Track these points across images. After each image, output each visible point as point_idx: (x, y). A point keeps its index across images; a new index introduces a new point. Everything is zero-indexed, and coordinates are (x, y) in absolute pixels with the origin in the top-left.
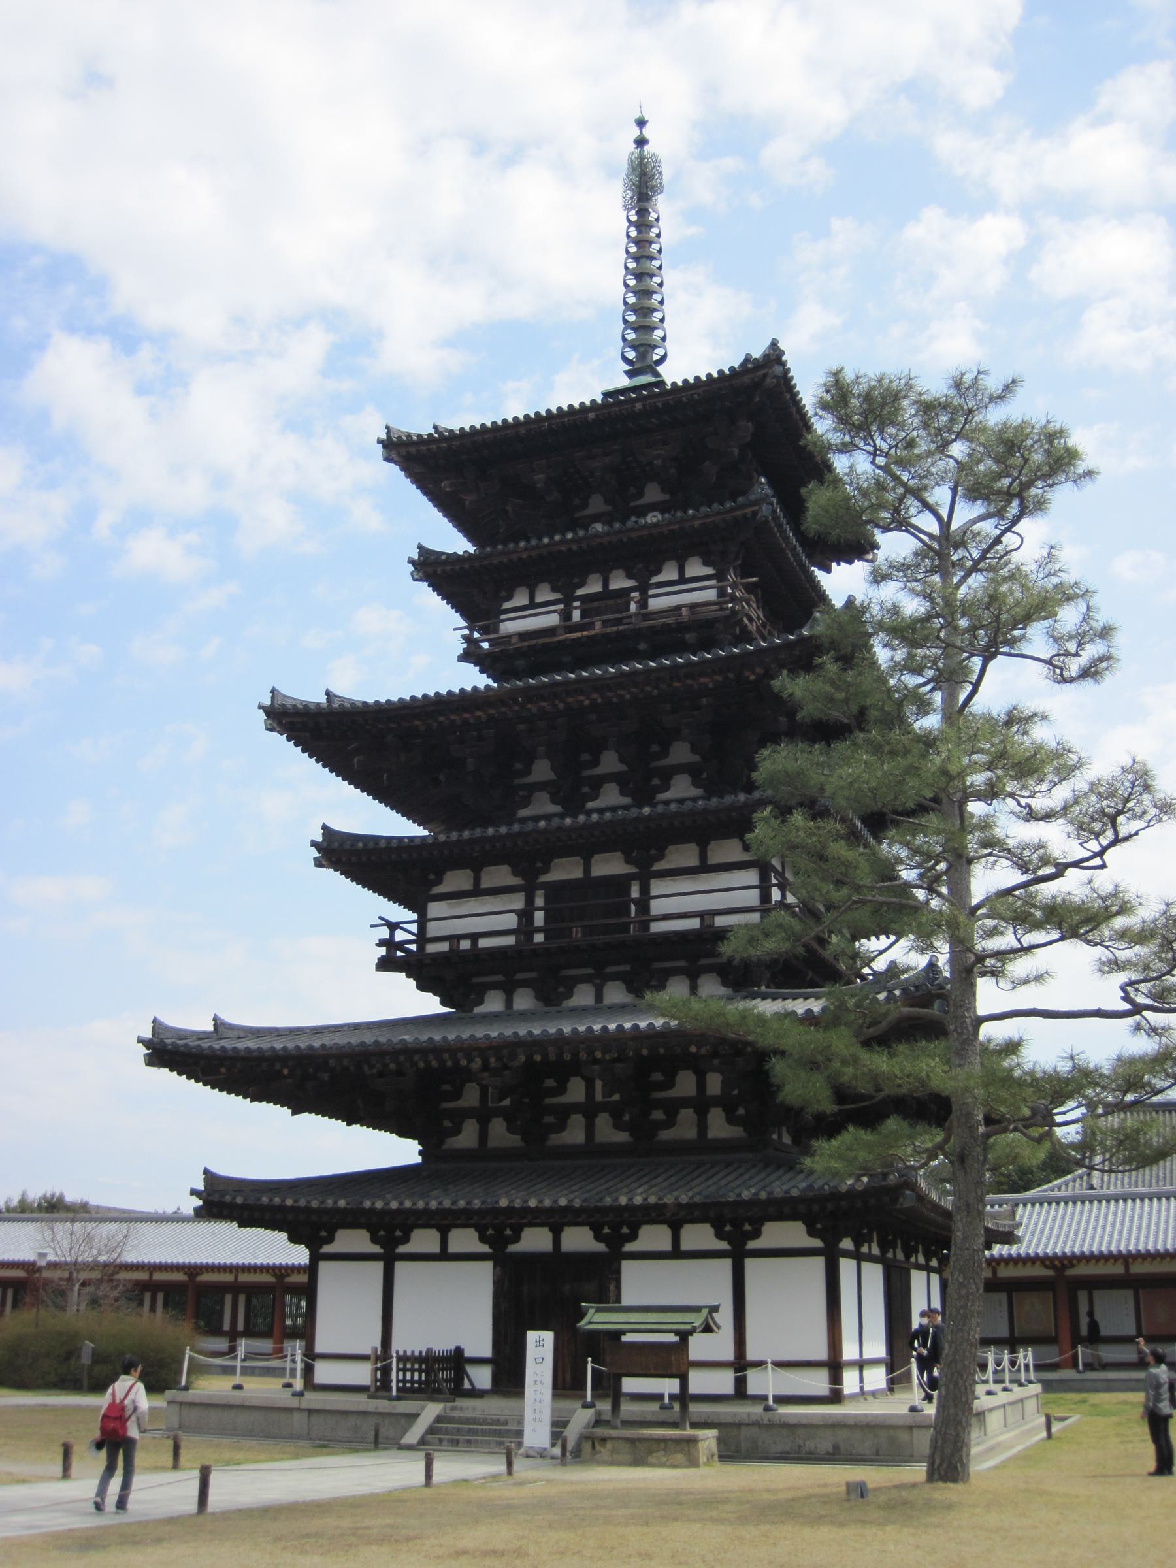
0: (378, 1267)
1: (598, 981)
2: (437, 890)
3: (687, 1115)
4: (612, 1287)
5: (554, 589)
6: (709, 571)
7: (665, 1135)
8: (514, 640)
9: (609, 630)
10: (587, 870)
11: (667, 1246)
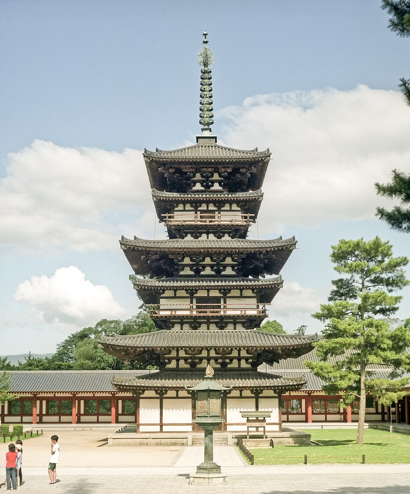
0: (158, 401)
1: (208, 324)
2: (162, 296)
3: (235, 361)
4: (224, 405)
5: (191, 206)
6: (239, 209)
7: (229, 366)
8: (182, 221)
9: (211, 223)
10: (208, 294)
11: (239, 395)
